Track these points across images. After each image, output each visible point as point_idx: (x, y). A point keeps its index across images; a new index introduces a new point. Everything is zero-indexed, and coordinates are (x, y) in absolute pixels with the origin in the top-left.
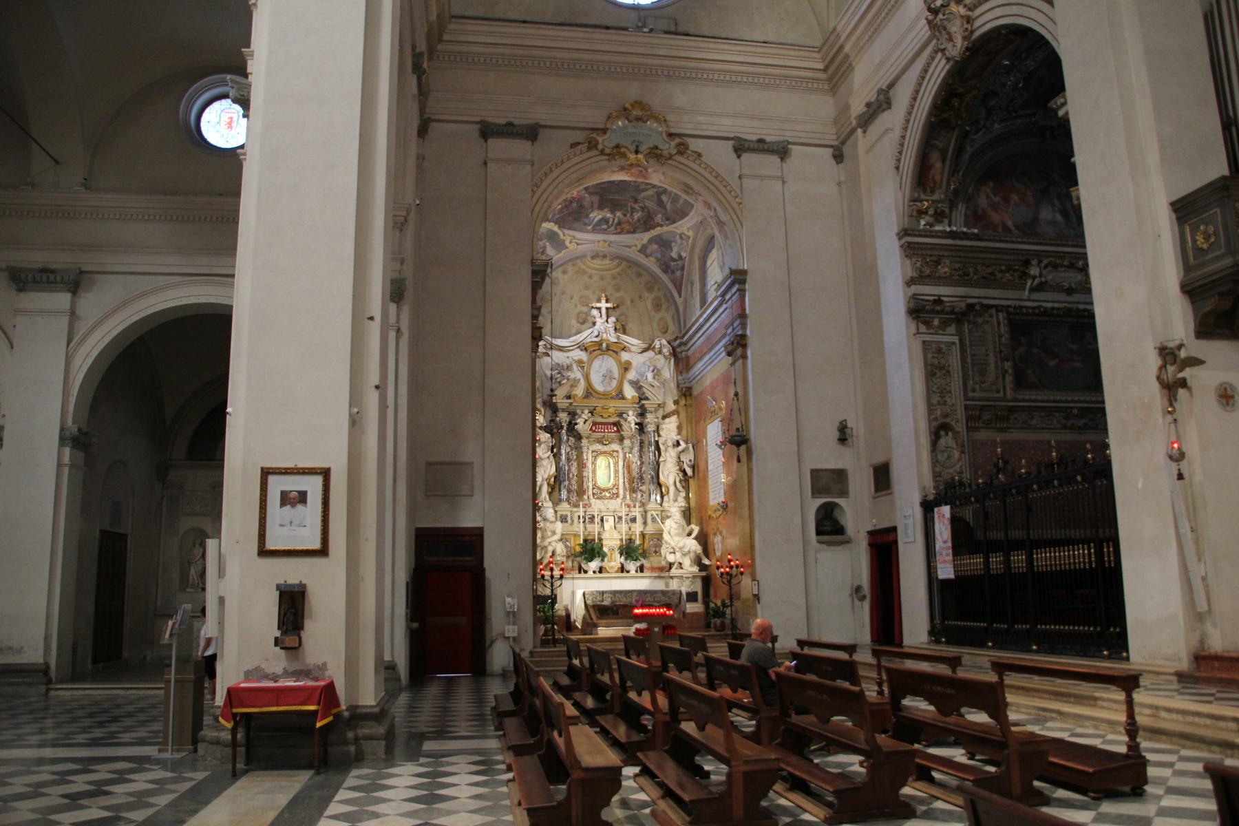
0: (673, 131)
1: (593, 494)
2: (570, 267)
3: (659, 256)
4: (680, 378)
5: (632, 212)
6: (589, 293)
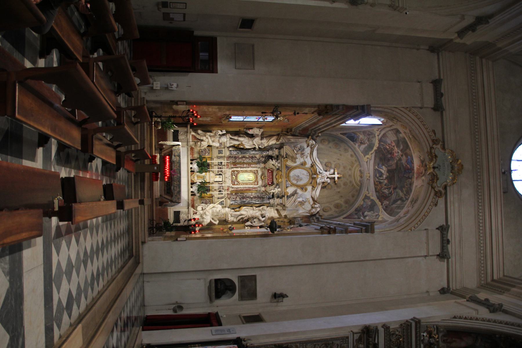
0: (448, 188)
1: (234, 171)
2: (354, 159)
3: (364, 206)
4: (299, 219)
5: (387, 188)
6: (341, 168)
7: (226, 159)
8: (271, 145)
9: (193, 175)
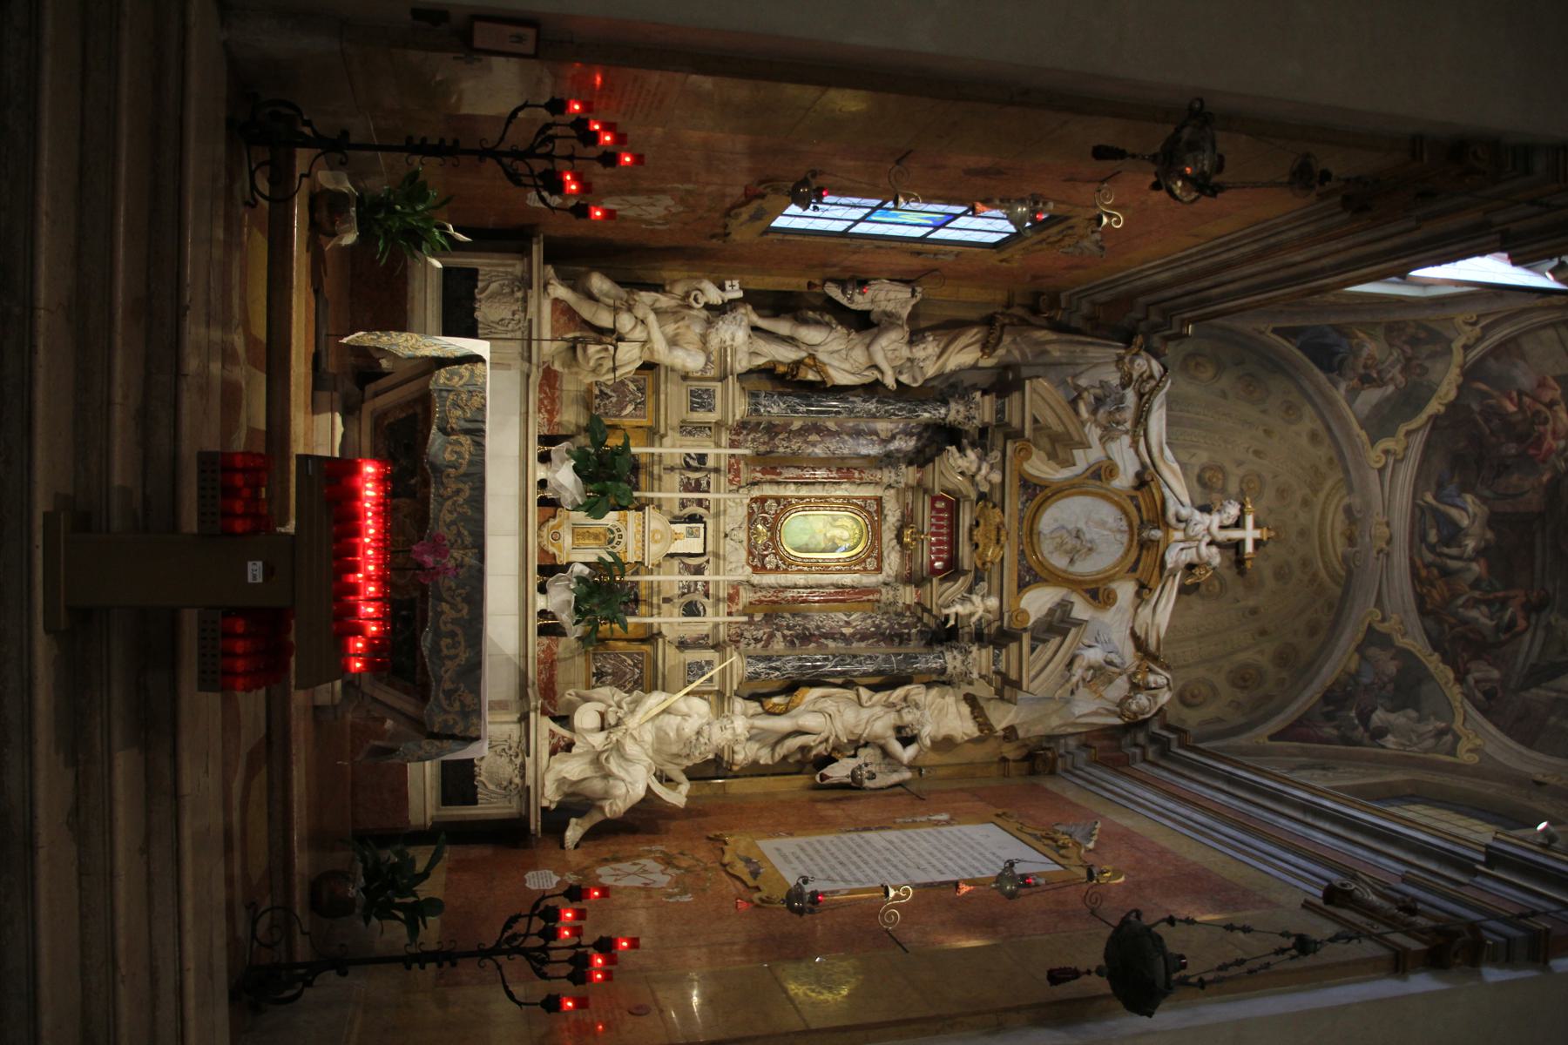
1: (763, 500)
2: (1323, 452)
3: (1365, 680)
4: (1072, 742)
5: (1488, 603)
7: (725, 438)
8: (953, 373)
9: (552, 523)
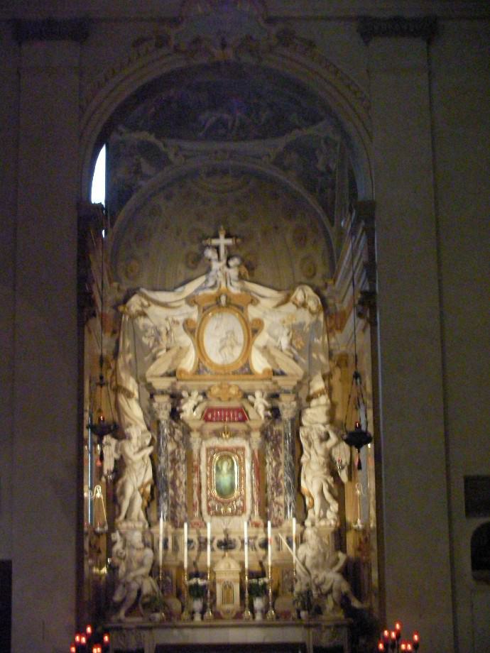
0: (272, 14)
1: (209, 509)
